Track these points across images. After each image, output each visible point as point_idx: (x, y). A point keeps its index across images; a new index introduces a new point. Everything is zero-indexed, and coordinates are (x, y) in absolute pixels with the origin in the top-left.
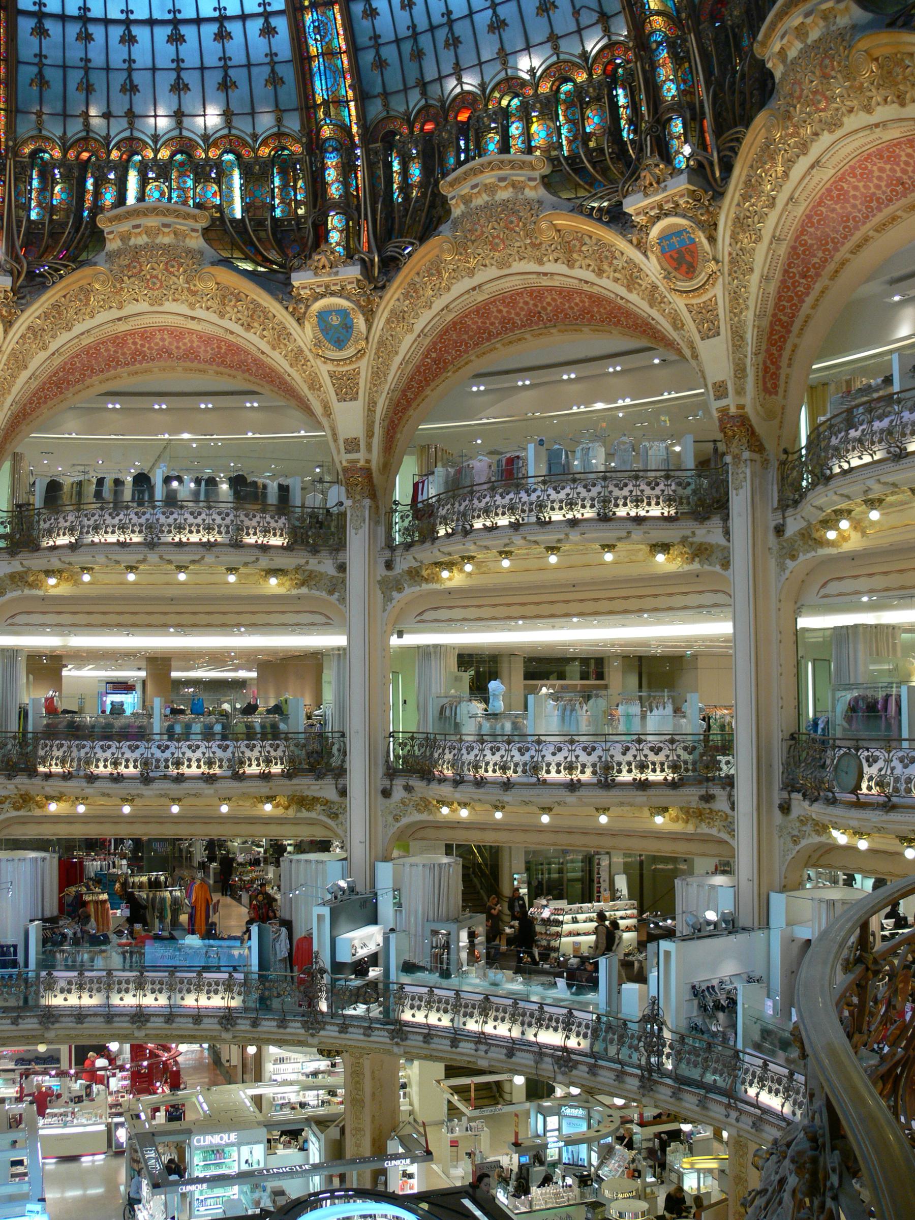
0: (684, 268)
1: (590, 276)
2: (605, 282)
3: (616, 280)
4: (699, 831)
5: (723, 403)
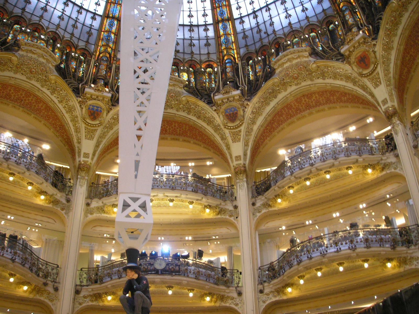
0: (93, 116)
1: (56, 101)
2: (60, 106)
3: (65, 107)
4: (35, 297)
5: (86, 159)
